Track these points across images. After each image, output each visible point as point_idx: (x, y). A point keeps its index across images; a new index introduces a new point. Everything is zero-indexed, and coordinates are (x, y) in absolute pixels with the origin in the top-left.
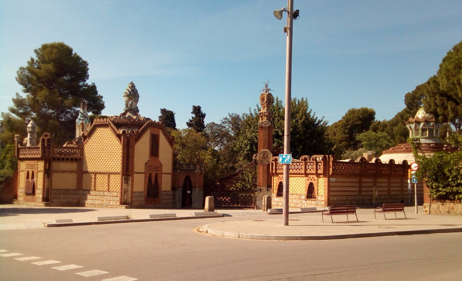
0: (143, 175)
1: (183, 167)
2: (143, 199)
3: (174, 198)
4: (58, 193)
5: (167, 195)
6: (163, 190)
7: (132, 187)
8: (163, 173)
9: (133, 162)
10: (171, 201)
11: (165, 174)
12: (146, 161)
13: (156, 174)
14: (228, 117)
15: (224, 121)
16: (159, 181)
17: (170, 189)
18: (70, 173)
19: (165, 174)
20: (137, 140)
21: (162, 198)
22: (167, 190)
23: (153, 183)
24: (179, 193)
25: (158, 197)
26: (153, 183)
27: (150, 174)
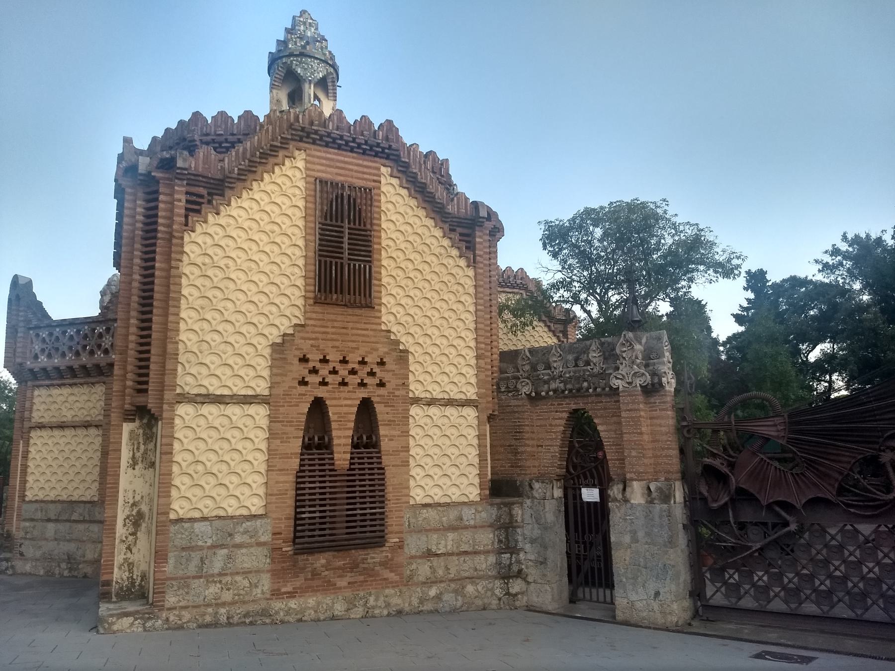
0: (260, 412)
1: (548, 367)
2: (254, 558)
3: (508, 546)
4: (39, 515)
5: (453, 528)
6: (418, 496)
7: (165, 486)
8: (416, 401)
9: (169, 332)
10: (486, 563)
11: (431, 402)
12: (285, 326)
13: (366, 408)
14: (844, 247)
15: (828, 259)
16: (385, 444)
17: (474, 493)
18: (81, 432)
19: (431, 402)
20: (196, 208)
21: (414, 545)
22: (455, 495)
23: (342, 455)
24: (542, 513)
25: (378, 540)
26: (342, 455)
27: (318, 407)
